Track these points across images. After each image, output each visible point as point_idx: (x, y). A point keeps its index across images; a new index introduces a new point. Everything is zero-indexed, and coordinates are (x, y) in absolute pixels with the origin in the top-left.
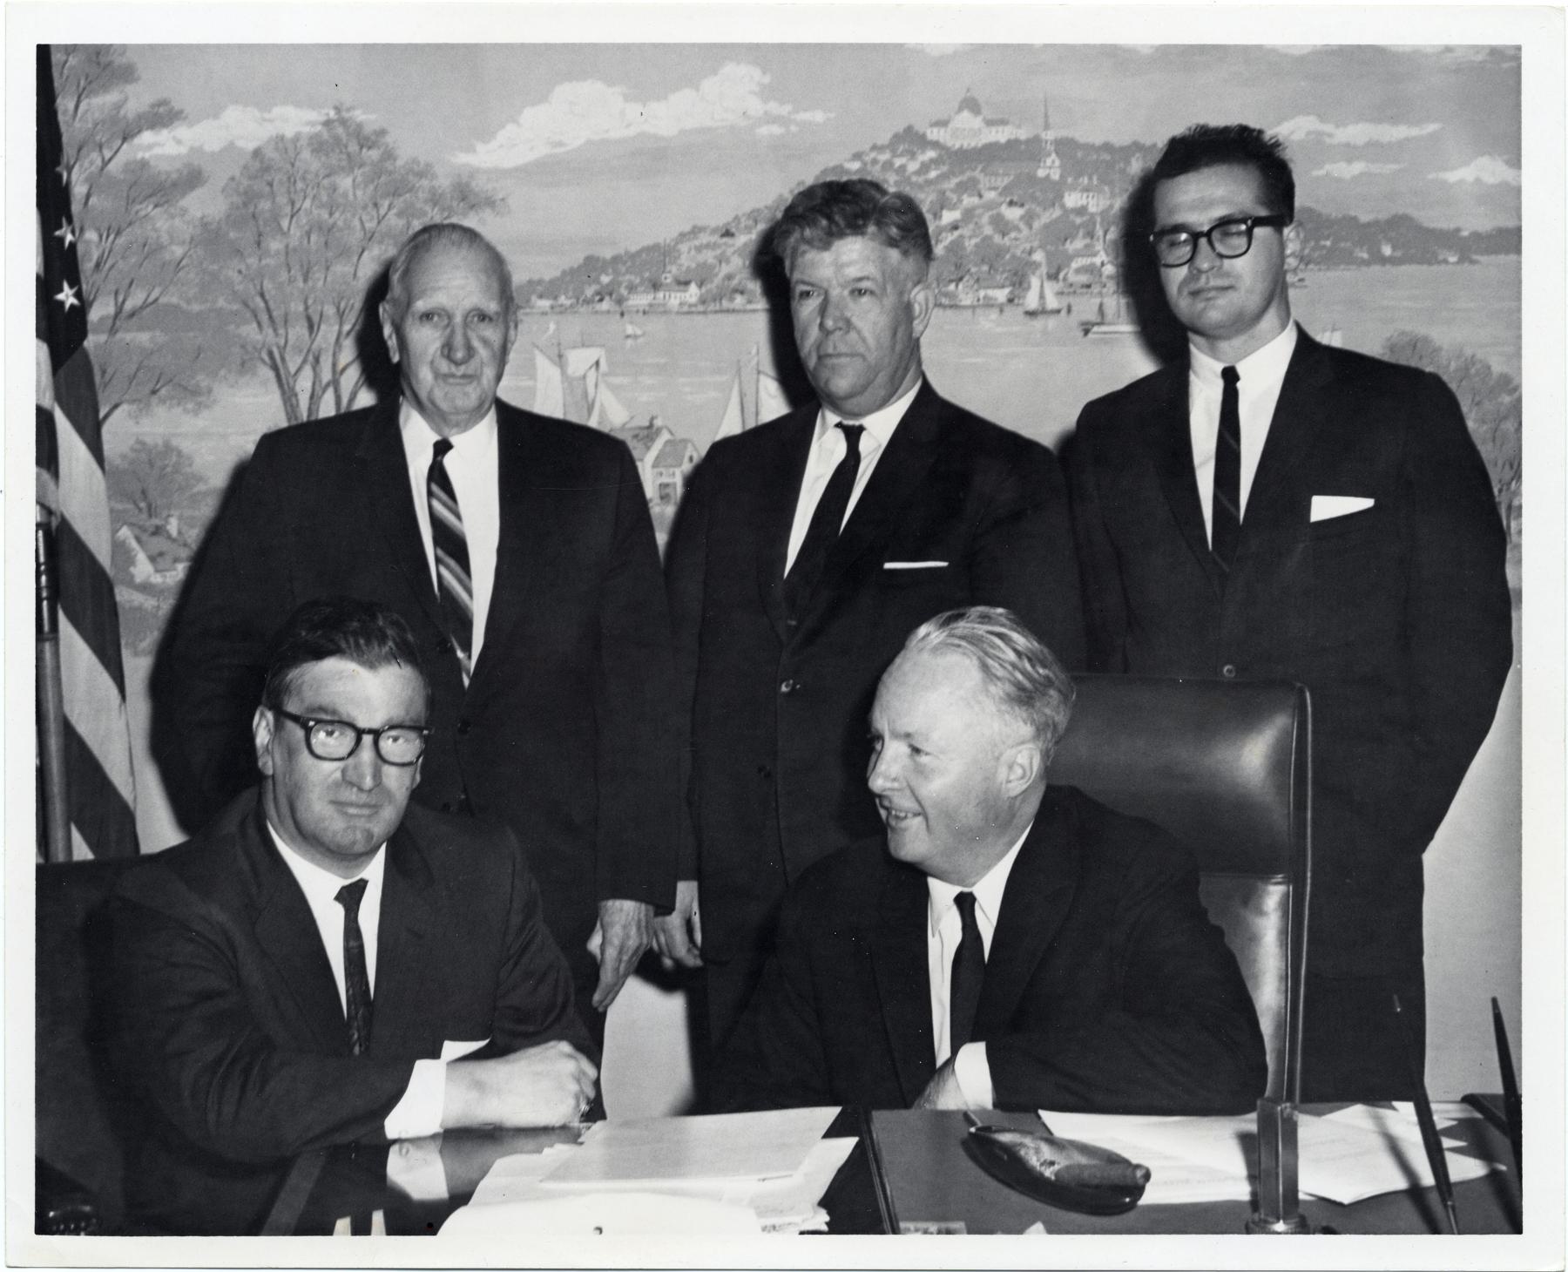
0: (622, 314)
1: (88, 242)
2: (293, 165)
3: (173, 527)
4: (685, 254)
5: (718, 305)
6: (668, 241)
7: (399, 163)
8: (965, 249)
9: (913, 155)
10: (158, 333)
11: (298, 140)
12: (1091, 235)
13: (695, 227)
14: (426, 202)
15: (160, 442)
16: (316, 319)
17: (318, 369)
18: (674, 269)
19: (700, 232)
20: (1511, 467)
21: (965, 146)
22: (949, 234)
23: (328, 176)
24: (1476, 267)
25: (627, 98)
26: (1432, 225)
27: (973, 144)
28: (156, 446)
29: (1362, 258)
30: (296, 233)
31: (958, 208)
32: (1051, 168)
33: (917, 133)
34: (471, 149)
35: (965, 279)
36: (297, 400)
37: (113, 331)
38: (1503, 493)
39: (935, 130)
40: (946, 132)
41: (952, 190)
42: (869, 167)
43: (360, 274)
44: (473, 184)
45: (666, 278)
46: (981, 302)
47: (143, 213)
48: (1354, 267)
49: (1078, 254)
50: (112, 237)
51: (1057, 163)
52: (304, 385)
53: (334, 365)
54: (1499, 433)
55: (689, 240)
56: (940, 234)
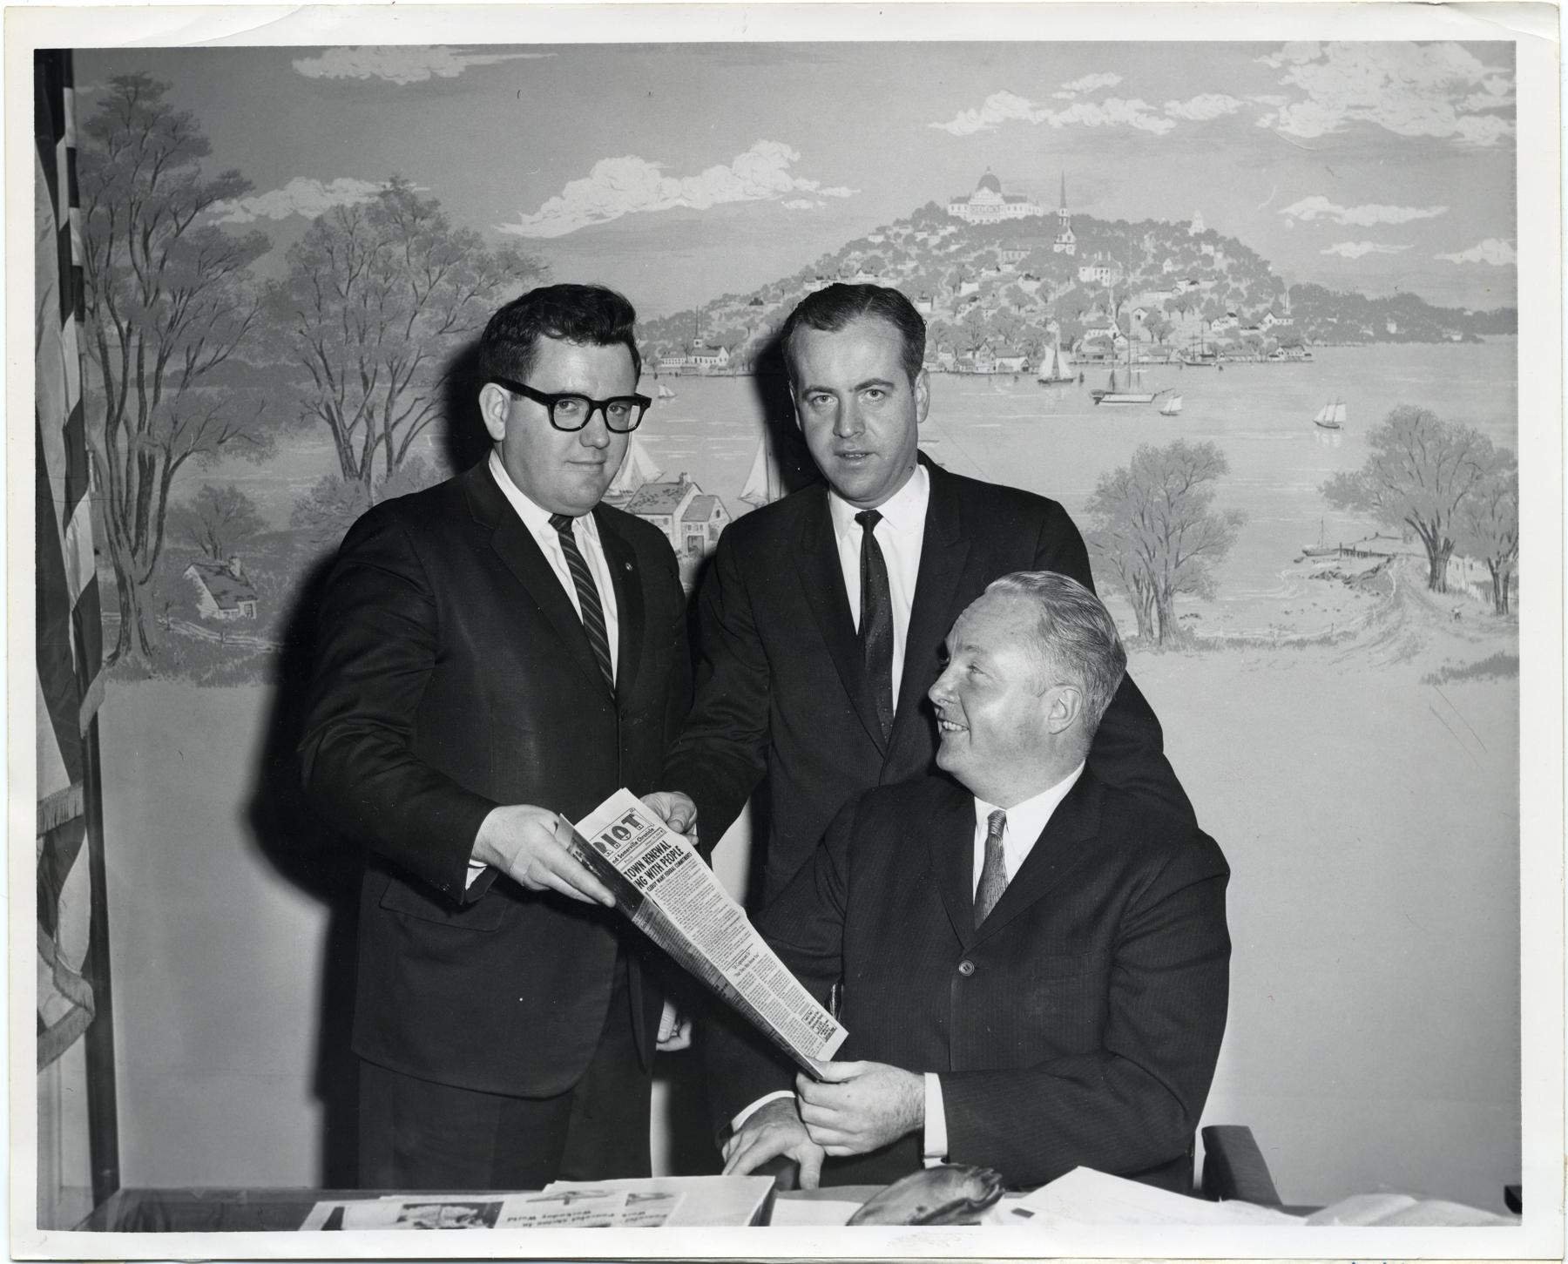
0: (656, 377)
1: (165, 302)
2: (351, 234)
3: (236, 569)
6: (700, 309)
7: (450, 232)
8: (982, 319)
9: (933, 231)
10: (225, 387)
11: (357, 210)
12: (1103, 308)
13: (725, 295)
14: (474, 268)
15: (226, 489)
16: (370, 376)
17: (372, 423)
18: (705, 334)
19: (730, 300)
20: (1510, 540)
21: (984, 223)
22: (968, 306)
23: (383, 244)
24: (1480, 346)
25: (664, 174)
26: (1436, 305)
27: (992, 220)
28: (223, 491)
29: (1369, 336)
30: (353, 298)
31: (975, 281)
32: (1066, 244)
33: (938, 208)
34: (519, 222)
35: (981, 349)
36: (352, 451)
37: (184, 385)
38: (1500, 566)
39: (956, 206)
40: (966, 208)
41: (972, 264)
42: (892, 241)
43: (412, 335)
44: (518, 253)
45: (697, 343)
46: (997, 370)
47: (213, 277)
48: (1360, 344)
49: (1091, 326)
50: (185, 298)
51: (1073, 239)
52: (358, 439)
53: (386, 420)
54: (1498, 508)
56: (959, 304)
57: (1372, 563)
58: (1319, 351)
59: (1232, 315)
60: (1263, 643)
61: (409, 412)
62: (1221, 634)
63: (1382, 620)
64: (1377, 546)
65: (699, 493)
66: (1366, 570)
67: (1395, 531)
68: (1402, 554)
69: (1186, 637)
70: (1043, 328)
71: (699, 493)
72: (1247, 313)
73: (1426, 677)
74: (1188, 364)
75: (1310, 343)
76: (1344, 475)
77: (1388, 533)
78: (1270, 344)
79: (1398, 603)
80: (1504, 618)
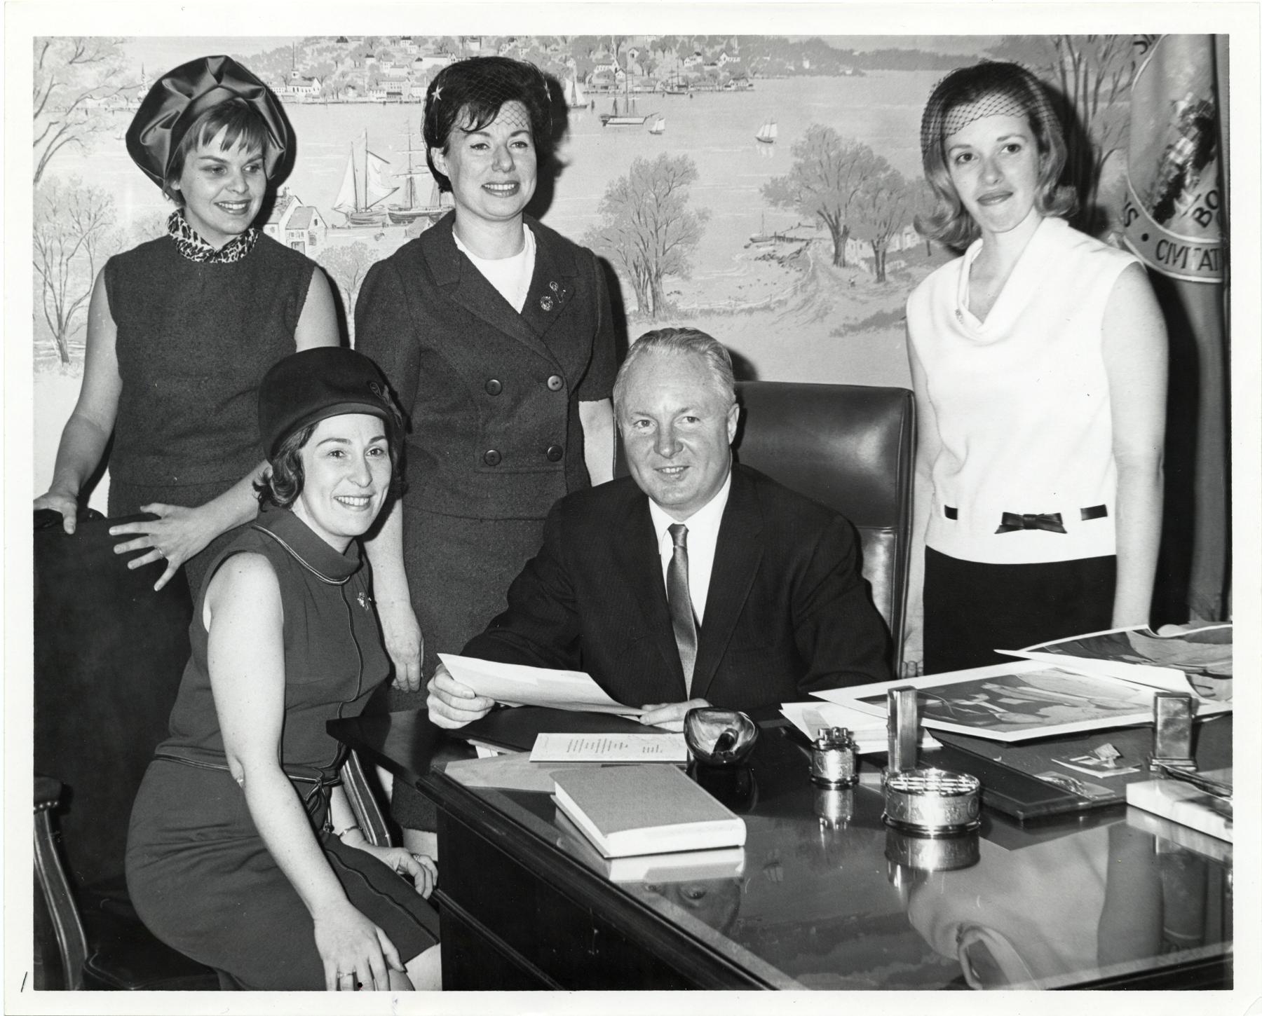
4: (310, 56)
5: (335, 96)
12: (608, 48)
18: (300, 67)
20: (885, 224)
22: (507, 45)
29: (791, 71)
38: (881, 245)
43: (45, 64)
45: (294, 75)
48: (785, 77)
54: (877, 200)
55: (313, 43)
56: (501, 44)
57: (796, 246)
58: (758, 82)
59: (698, 54)
60: (724, 312)
61: (44, 135)
62: (695, 306)
63: (804, 289)
64: (801, 233)
65: (299, 204)
66: (792, 252)
67: (811, 221)
68: (816, 239)
69: (671, 309)
70: (561, 63)
71: (301, 205)
72: (709, 53)
73: (833, 331)
74: (669, 93)
75: (752, 76)
76: (777, 179)
77: (805, 224)
78: (725, 77)
79: (814, 277)
80: (882, 284)
